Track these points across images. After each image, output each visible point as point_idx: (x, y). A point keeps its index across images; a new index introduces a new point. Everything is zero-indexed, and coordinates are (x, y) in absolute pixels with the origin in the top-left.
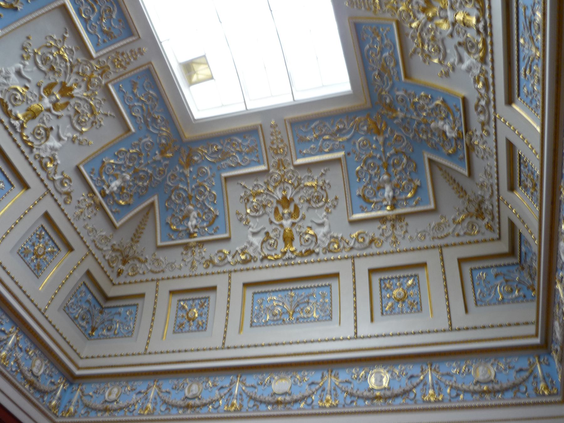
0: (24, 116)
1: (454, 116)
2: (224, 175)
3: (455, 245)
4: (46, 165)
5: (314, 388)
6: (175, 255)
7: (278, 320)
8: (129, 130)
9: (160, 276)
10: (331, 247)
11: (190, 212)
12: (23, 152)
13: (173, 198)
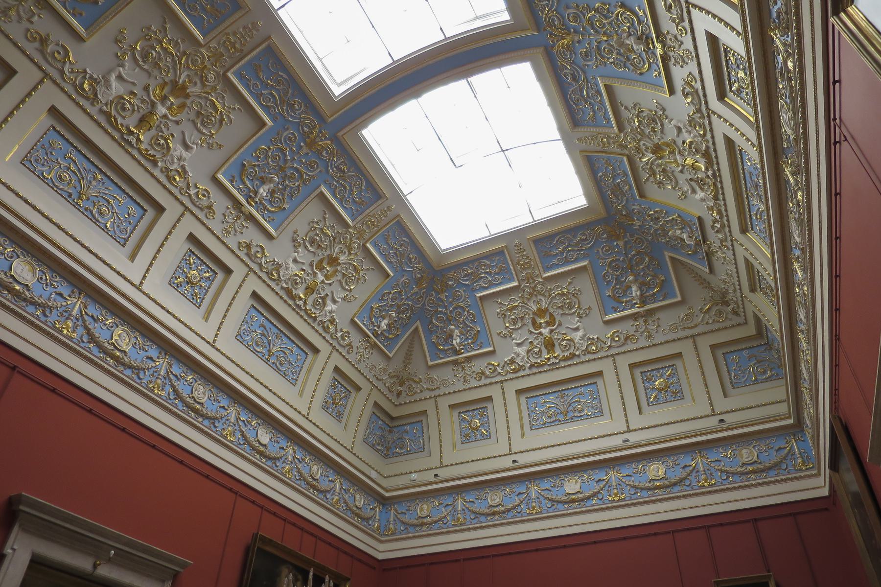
0: (305, 295)
1: (690, 228)
2: (478, 295)
3: (705, 333)
4: (328, 327)
5: (602, 485)
6: (447, 373)
7: (554, 421)
8: (388, 275)
9: (437, 393)
10: (589, 349)
11: (452, 331)
12: (309, 324)
13: (434, 321)
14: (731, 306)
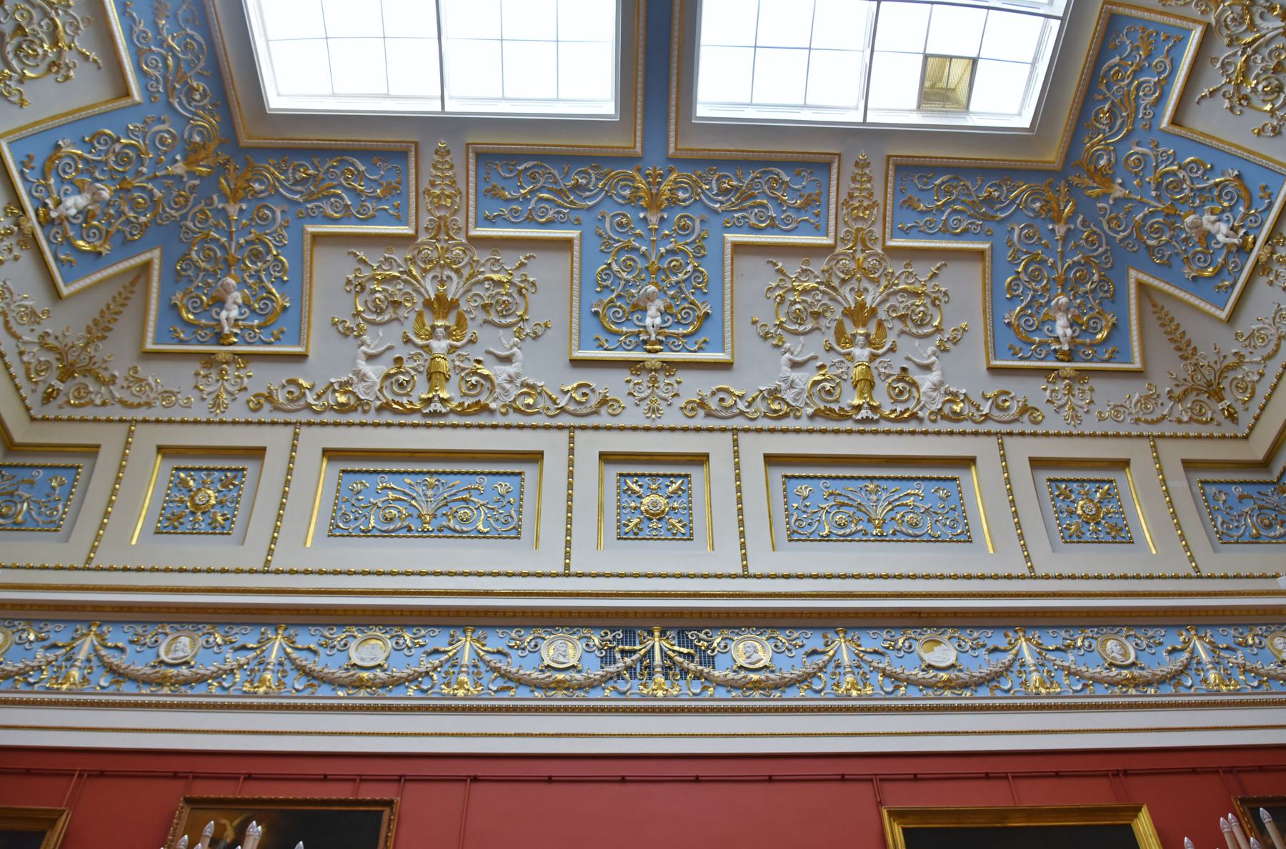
14: (61, 386)
